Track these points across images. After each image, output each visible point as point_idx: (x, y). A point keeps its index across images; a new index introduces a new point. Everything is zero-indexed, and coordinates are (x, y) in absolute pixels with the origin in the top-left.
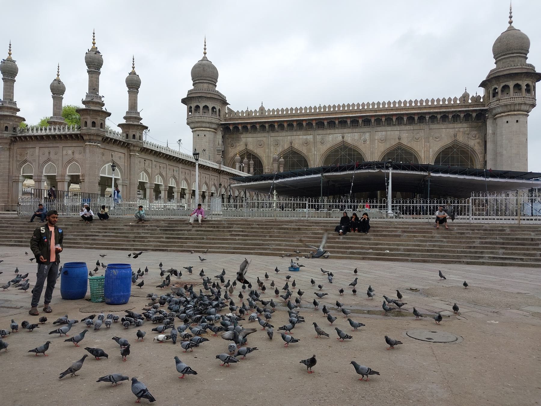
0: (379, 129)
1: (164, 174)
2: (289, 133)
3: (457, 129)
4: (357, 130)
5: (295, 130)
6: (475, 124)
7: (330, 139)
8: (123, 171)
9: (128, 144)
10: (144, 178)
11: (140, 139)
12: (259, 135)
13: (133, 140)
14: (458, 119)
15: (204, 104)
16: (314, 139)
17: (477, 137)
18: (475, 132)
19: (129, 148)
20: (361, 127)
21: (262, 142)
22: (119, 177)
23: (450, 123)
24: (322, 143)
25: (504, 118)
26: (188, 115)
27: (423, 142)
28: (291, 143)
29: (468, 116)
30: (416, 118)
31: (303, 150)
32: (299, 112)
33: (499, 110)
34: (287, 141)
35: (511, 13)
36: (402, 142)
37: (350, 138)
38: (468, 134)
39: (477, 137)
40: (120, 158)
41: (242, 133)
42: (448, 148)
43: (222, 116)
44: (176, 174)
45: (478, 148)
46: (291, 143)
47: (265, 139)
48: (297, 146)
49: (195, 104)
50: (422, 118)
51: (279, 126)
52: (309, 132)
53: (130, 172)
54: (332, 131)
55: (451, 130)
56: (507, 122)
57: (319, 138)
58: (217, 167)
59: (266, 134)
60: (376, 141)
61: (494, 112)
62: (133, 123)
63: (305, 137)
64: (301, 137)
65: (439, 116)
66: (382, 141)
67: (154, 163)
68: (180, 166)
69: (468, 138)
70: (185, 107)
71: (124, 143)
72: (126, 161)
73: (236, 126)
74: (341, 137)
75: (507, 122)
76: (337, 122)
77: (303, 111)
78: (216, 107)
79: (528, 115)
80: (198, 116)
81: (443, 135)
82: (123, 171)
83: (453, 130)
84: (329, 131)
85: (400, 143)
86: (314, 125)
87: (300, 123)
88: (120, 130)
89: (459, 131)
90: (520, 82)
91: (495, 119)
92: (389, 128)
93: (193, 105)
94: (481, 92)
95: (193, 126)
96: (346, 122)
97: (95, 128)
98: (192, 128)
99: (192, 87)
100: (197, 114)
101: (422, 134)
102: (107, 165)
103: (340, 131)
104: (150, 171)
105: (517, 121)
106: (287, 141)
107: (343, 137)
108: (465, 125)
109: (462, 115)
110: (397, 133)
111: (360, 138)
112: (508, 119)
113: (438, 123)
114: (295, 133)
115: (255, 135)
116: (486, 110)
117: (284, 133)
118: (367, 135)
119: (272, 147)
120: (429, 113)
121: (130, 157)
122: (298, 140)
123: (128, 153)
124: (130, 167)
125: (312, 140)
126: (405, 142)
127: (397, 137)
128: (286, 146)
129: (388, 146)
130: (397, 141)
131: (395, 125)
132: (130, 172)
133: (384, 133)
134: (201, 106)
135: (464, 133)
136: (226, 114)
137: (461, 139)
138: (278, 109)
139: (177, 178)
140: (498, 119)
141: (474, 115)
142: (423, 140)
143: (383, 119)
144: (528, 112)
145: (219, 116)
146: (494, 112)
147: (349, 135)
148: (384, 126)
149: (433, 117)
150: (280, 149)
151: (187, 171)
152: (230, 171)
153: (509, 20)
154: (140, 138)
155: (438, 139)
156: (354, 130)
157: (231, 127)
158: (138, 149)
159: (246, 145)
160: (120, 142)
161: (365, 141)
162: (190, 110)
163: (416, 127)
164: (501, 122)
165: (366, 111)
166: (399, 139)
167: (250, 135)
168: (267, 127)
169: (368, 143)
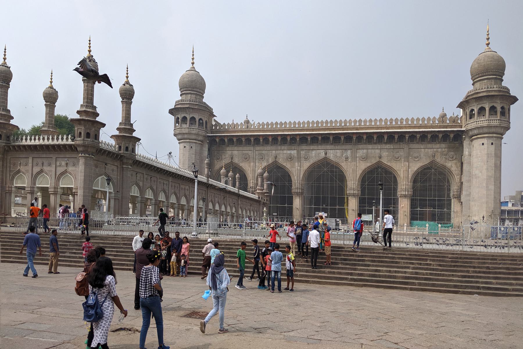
0: (360, 146)
1: (155, 188)
2: (274, 147)
3: (435, 150)
4: (339, 147)
5: (281, 145)
6: (453, 145)
7: (314, 155)
8: (116, 184)
9: (121, 156)
10: (135, 192)
11: (133, 152)
12: (245, 148)
13: (127, 152)
14: (436, 139)
16: (298, 154)
17: (454, 158)
18: (452, 153)
19: (121, 161)
20: (343, 144)
21: (247, 156)
22: (112, 191)
23: (429, 143)
24: (306, 159)
25: (479, 140)
26: (175, 126)
27: (403, 161)
28: (276, 157)
29: (445, 137)
31: (288, 165)
32: (283, 126)
33: (476, 132)
34: (272, 155)
37: (332, 155)
39: (454, 158)
40: (113, 170)
41: (228, 146)
43: (209, 128)
44: (166, 187)
46: (276, 157)
47: (250, 152)
50: (401, 136)
51: (263, 140)
52: (293, 147)
53: (122, 184)
54: (315, 147)
55: (429, 150)
56: (483, 144)
57: (303, 153)
58: (205, 181)
59: (252, 148)
60: (358, 159)
61: (471, 133)
62: (127, 136)
63: (289, 152)
64: (285, 152)
67: (146, 176)
68: (171, 179)
69: (446, 159)
71: (117, 155)
72: (119, 174)
73: (222, 139)
74: (324, 153)
75: (483, 144)
76: (320, 138)
77: (288, 126)
78: (203, 119)
79: (502, 138)
80: (185, 128)
81: (422, 155)
82: (116, 184)
83: (432, 150)
84: (312, 147)
85: (379, 162)
86: (298, 140)
87: (284, 138)
88: (113, 142)
89: (437, 151)
91: (472, 141)
92: (370, 146)
95: (180, 137)
96: (328, 138)
97: (89, 140)
98: (179, 140)
100: (184, 126)
101: (402, 153)
102: (100, 178)
103: (323, 147)
104: (141, 184)
105: (492, 144)
106: (272, 155)
107: (326, 154)
108: (443, 145)
110: (378, 151)
111: (342, 155)
112: (485, 141)
113: (417, 143)
114: (279, 148)
115: (241, 148)
116: (463, 131)
117: (269, 148)
118: (349, 152)
119: (257, 161)
121: (123, 170)
122: (282, 155)
123: (120, 165)
124: (123, 181)
125: (296, 155)
126: (385, 161)
128: (270, 161)
129: (369, 164)
130: (378, 159)
131: (376, 143)
132: (122, 184)
133: (365, 151)
135: (442, 154)
136: (213, 125)
137: (439, 160)
138: (263, 123)
139: (167, 191)
140: (474, 141)
141: (452, 136)
142: (403, 159)
143: (365, 137)
144: (502, 134)
145: (206, 127)
146: (471, 133)
147: (332, 151)
148: (365, 144)
149: (413, 136)
151: (177, 185)
152: (252, 197)
154: (133, 150)
155: (418, 159)
156: (337, 148)
157: (217, 140)
158: (131, 162)
160: (114, 154)
161: (347, 158)
162: (177, 121)
163: (397, 146)
164: (477, 143)
165: (348, 129)
166: (380, 157)
168: (252, 141)
169: (349, 160)
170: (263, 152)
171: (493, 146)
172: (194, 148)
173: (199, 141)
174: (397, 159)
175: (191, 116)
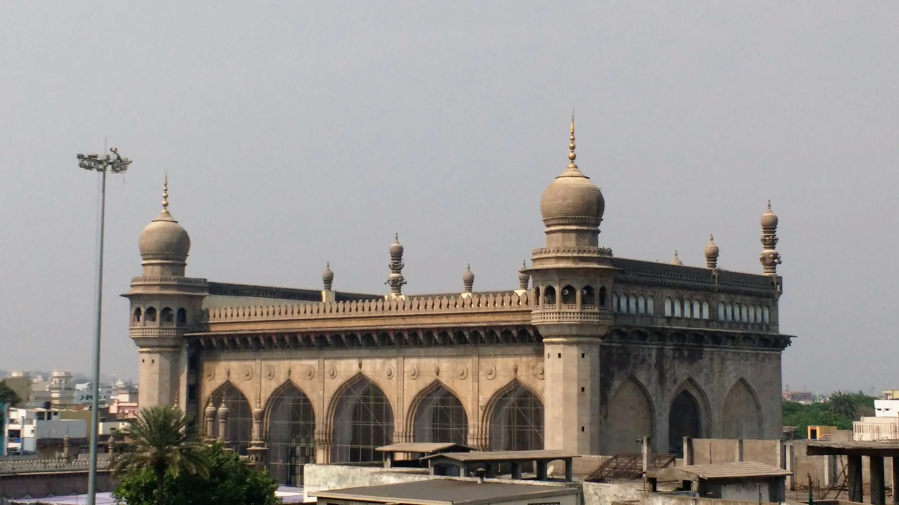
4: (378, 352)
15: (148, 306)
28: (290, 372)
36: (440, 379)
38: (533, 368)
46: (290, 372)
48: (298, 380)
60: (406, 375)
66: (416, 374)
81: (498, 368)
95: (142, 342)
99: (140, 272)
105: (560, 355)
107: (360, 365)
114: (294, 353)
118: (393, 363)
119: (263, 380)
126: (445, 380)
127: (433, 369)
129: (421, 386)
142: (470, 376)
150: (274, 385)
159: (229, 373)
166: (438, 374)
167: (233, 355)
170: (273, 363)
171: (561, 359)
172: (157, 361)
173: (167, 347)
174: (463, 375)
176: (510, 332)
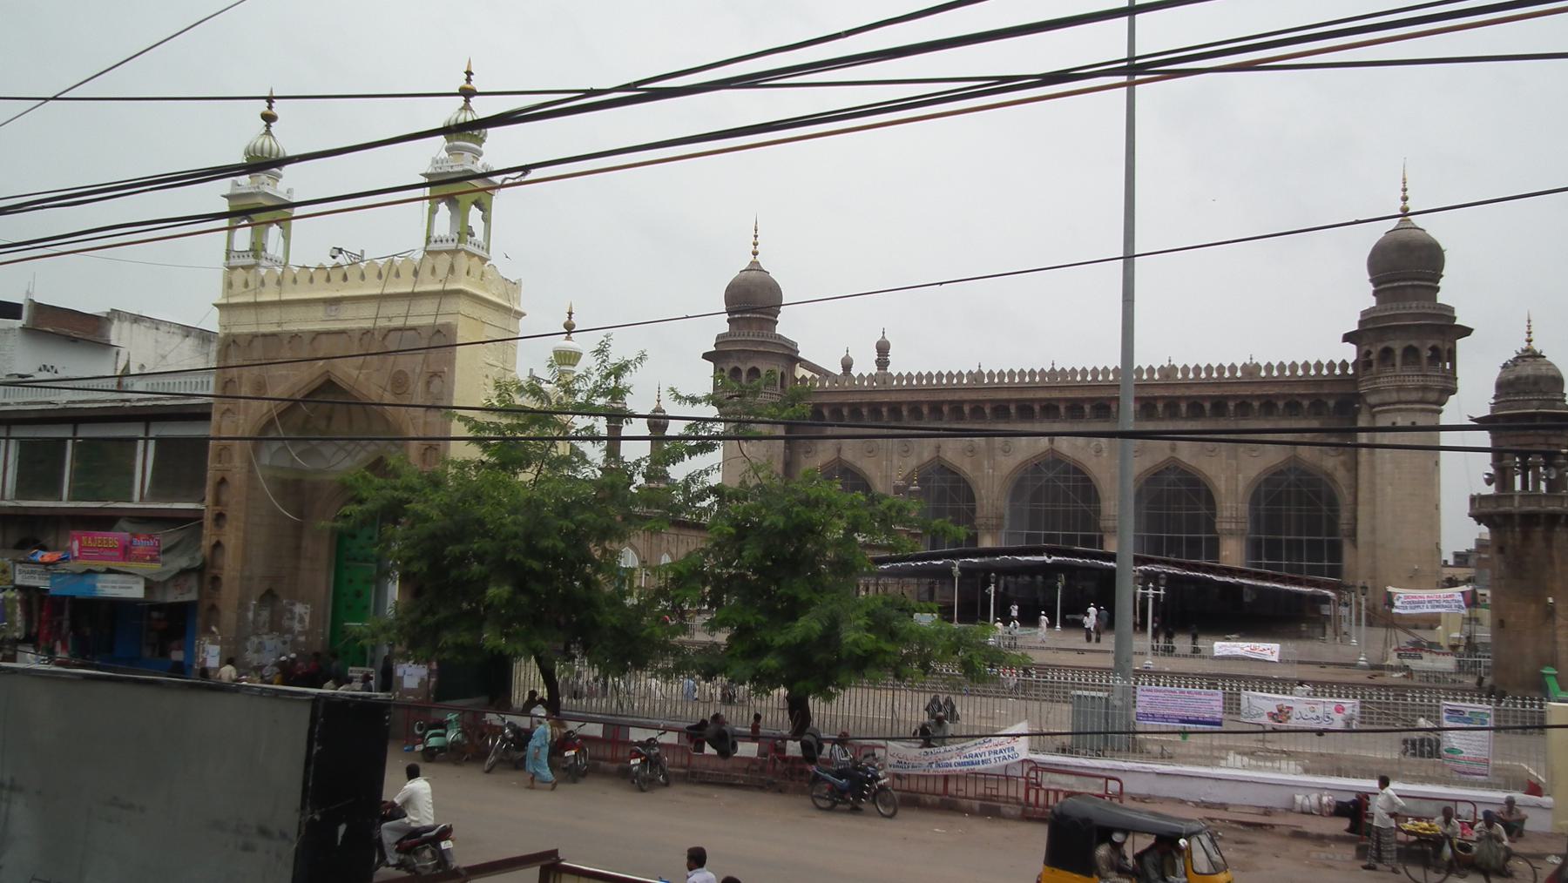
29: (1318, 405)
30: (1207, 406)
35: (1405, 190)
42: (1281, 472)
45: (1341, 476)
49: (732, 365)
65: (1256, 404)
70: (710, 366)
90: (1390, 344)
93: (728, 367)
94: (1350, 353)
109: (1306, 403)
120: (1235, 397)
134: (745, 368)
153: (1401, 204)
162: (718, 371)
175: (750, 365)
176: (1299, 405)
